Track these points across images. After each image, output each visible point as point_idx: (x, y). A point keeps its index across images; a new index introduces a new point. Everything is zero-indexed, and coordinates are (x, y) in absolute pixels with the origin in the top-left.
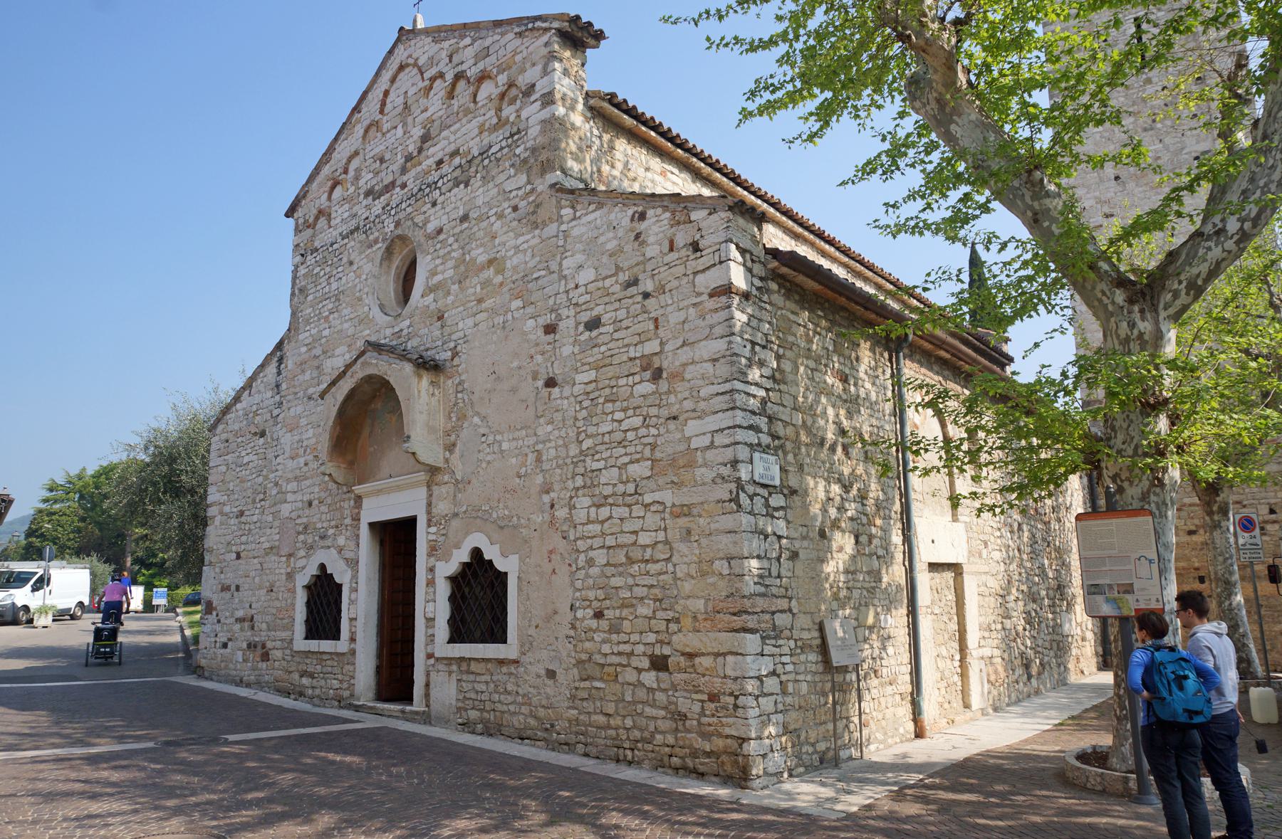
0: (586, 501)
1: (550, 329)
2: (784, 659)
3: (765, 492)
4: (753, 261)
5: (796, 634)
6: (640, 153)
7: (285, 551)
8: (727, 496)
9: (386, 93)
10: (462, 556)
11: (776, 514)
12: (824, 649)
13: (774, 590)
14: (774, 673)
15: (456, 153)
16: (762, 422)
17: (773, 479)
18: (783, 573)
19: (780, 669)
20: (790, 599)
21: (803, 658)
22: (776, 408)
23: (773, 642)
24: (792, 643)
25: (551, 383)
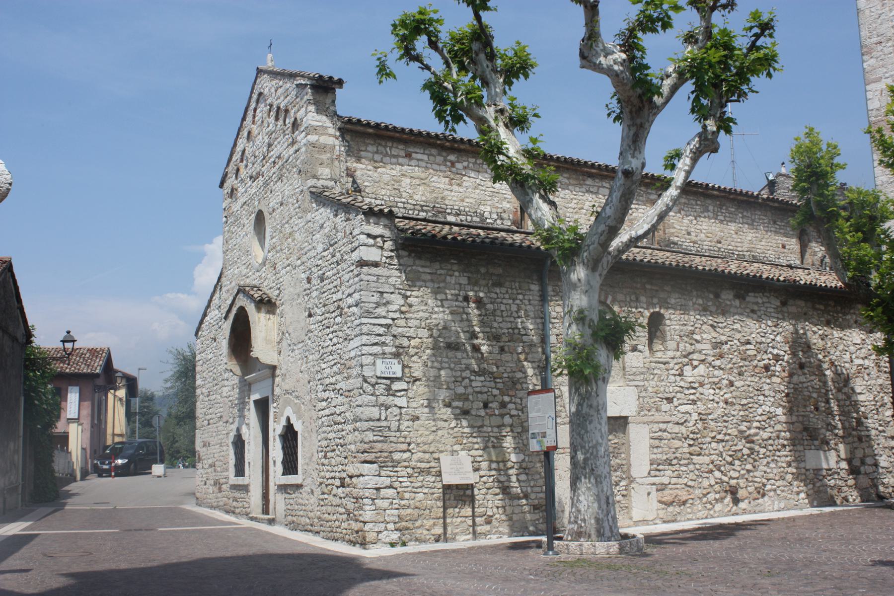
0: (321, 388)
1: (309, 280)
2: (400, 479)
3: (388, 382)
4: (384, 242)
5: (413, 463)
6: (385, 147)
7: (225, 419)
8: (359, 385)
9: (255, 110)
10: (283, 422)
11: (399, 394)
12: (439, 474)
13: (392, 439)
14: (391, 487)
15: (279, 157)
16: (388, 339)
17: (395, 373)
18: (402, 428)
19: (396, 484)
20: (409, 444)
21: (421, 478)
22: (400, 330)
23: (391, 469)
24: (409, 470)
25: (310, 315)
